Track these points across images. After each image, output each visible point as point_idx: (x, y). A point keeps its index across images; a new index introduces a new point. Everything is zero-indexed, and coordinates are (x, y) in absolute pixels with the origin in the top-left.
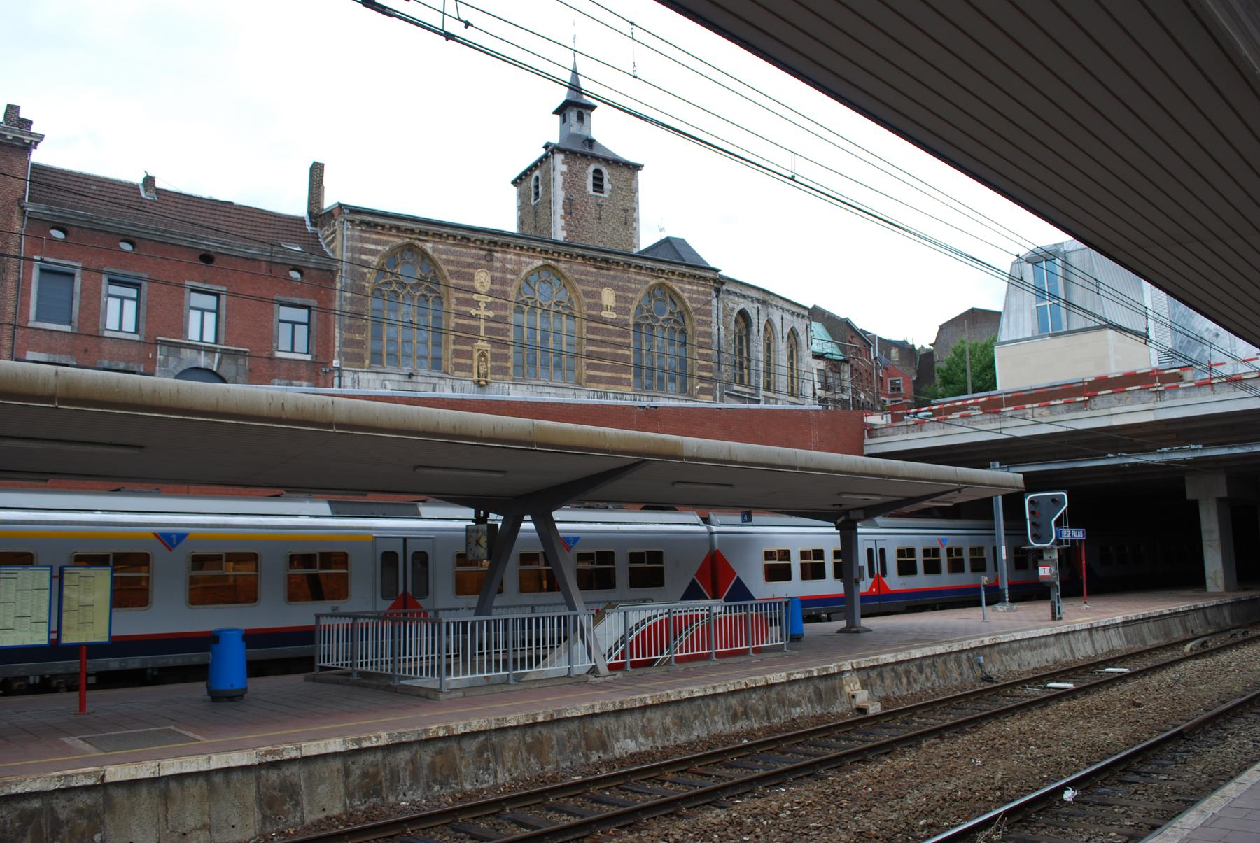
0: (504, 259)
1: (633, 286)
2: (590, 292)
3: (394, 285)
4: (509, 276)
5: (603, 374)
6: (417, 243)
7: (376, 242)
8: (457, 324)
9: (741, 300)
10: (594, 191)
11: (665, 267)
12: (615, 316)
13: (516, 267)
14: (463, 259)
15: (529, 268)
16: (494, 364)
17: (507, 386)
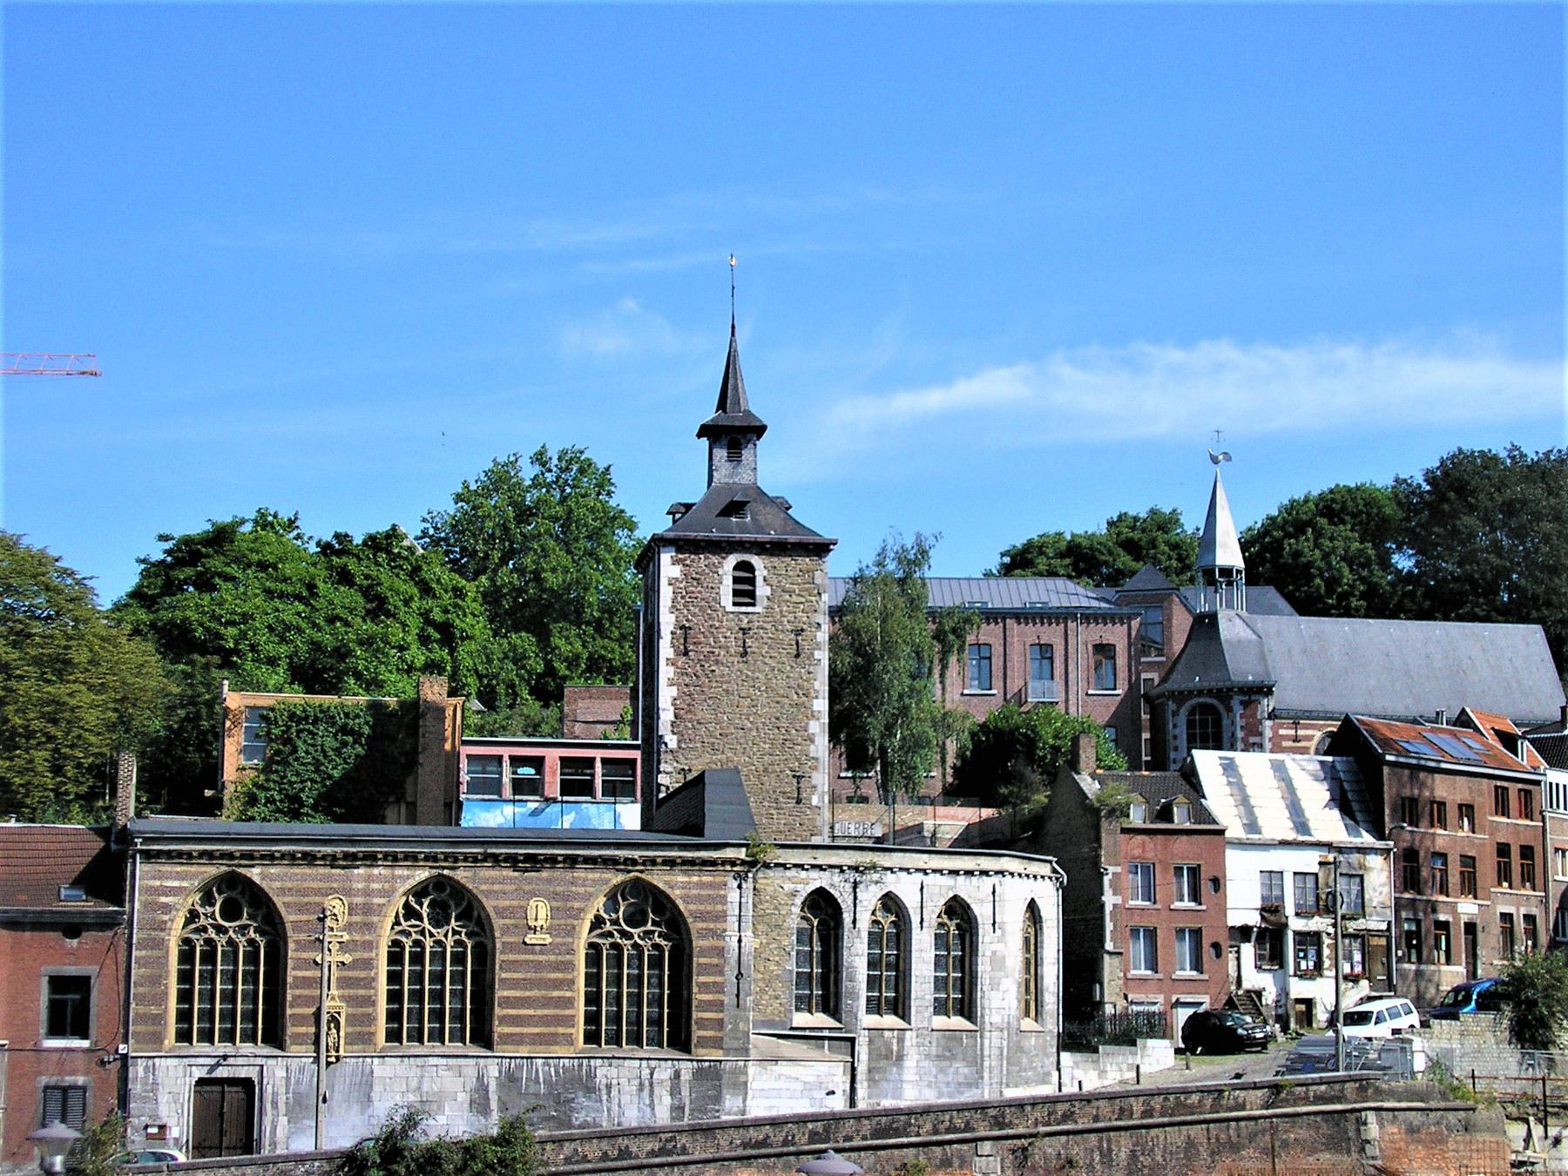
0: (369, 876)
1: (582, 890)
2: (506, 909)
3: (210, 930)
4: (376, 901)
5: (526, 1030)
6: (241, 870)
7: (179, 876)
8: (295, 978)
9: (814, 874)
10: (735, 604)
11: (636, 854)
12: (548, 940)
13: (387, 886)
14: (306, 885)
15: (408, 886)
16: (350, 1030)
17: (369, 1060)
